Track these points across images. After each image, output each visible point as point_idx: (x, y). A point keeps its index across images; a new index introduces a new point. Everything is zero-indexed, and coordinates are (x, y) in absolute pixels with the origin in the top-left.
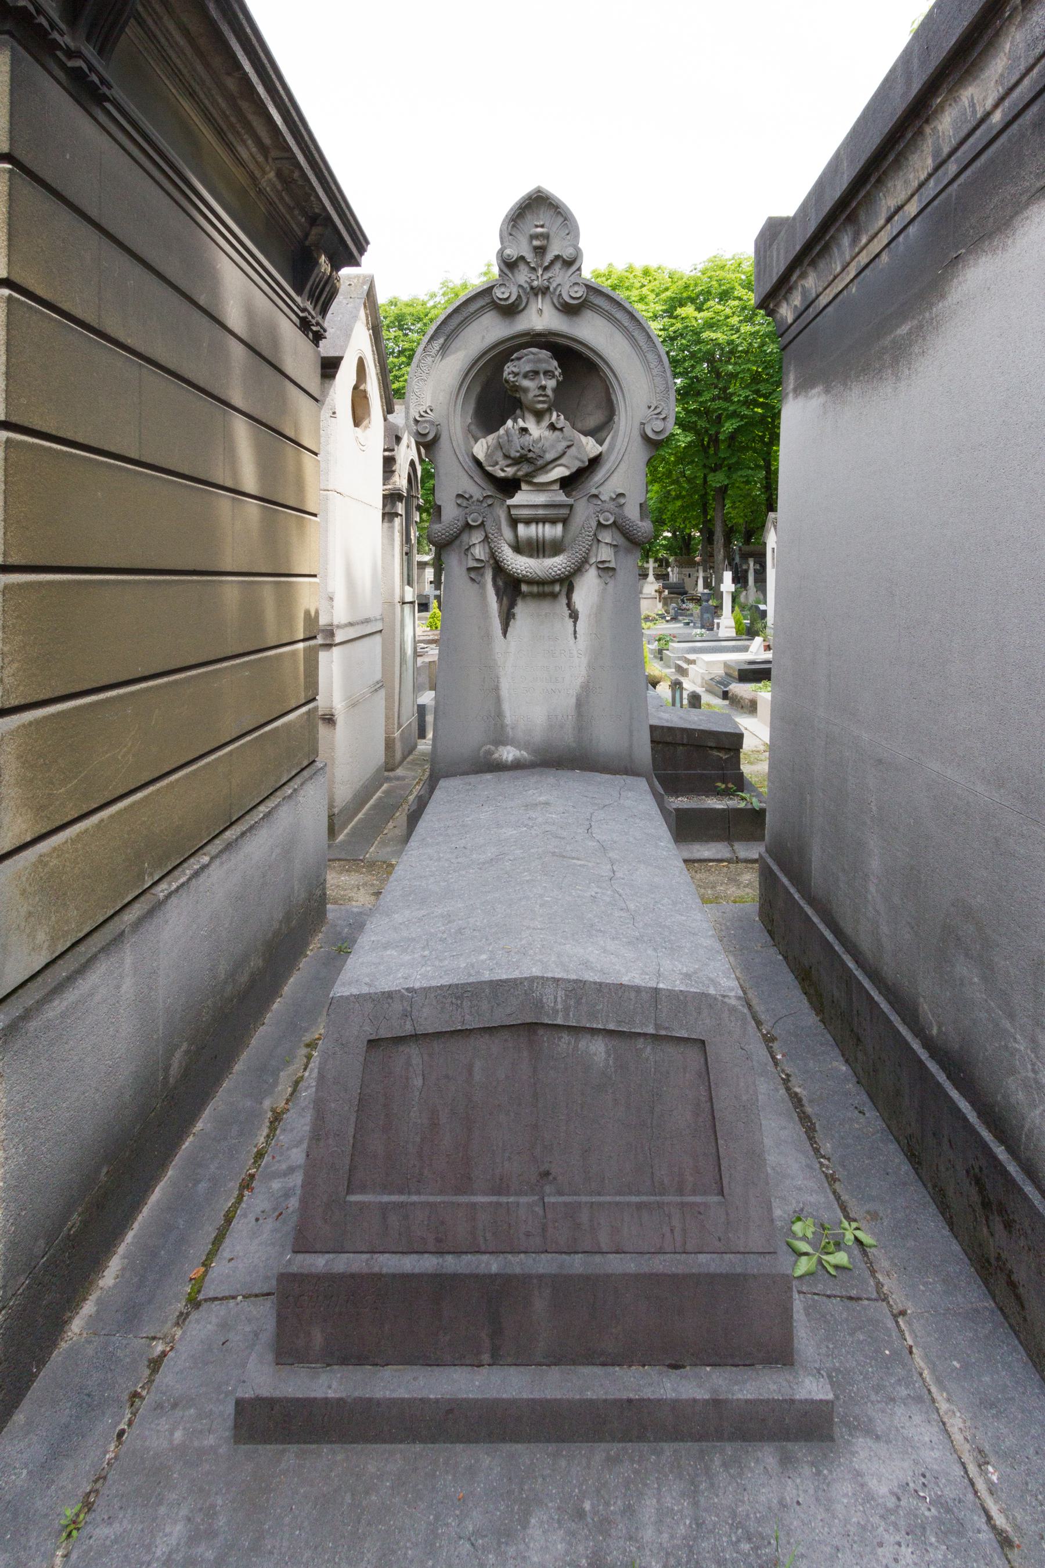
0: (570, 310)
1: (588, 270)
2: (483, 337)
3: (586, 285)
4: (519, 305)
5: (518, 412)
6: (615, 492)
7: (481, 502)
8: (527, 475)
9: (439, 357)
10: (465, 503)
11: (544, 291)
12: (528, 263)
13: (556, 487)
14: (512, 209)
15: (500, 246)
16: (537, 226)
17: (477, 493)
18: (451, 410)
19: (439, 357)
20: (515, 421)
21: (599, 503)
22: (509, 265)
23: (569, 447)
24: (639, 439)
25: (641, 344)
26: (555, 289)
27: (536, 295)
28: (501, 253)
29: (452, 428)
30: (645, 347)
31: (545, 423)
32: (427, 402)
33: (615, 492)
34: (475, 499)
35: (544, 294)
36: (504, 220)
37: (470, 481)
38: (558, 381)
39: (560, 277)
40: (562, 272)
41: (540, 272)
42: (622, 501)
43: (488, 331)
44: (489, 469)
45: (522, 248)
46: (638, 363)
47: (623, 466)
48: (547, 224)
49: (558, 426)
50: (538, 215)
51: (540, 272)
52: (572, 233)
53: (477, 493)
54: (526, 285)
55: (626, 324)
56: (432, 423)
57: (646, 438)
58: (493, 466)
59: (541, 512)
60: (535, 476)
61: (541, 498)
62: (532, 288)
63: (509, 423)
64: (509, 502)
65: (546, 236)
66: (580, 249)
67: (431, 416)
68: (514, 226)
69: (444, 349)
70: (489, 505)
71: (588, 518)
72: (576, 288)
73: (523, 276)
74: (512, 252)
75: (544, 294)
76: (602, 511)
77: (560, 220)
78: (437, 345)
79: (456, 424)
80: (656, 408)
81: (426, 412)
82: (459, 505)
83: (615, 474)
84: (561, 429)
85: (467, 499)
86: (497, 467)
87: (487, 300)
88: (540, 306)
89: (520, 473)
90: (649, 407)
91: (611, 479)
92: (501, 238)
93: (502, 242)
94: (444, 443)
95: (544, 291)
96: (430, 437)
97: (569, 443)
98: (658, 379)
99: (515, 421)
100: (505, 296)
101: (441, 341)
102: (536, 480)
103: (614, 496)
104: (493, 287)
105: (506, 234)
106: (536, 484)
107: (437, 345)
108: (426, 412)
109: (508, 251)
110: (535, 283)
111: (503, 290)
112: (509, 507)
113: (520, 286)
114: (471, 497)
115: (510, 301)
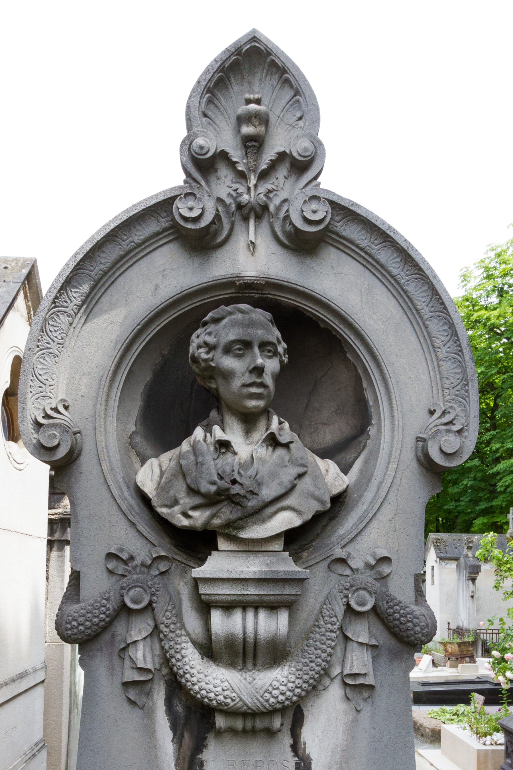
0: (303, 244)
1: (336, 179)
2: (157, 286)
3: (332, 203)
4: (216, 233)
5: (214, 414)
6: (374, 555)
7: (149, 567)
8: (229, 524)
9: (80, 317)
10: (121, 569)
11: (259, 212)
12: (233, 165)
13: (278, 546)
14: (207, 71)
15: (185, 133)
16: (248, 102)
17: (142, 552)
18: (101, 408)
19: (80, 317)
20: (208, 429)
21: (348, 572)
22: (202, 165)
23: (300, 476)
24: (414, 465)
25: (420, 305)
26: (278, 208)
27: (246, 219)
28: (187, 144)
29: (101, 438)
30: (426, 311)
31: (260, 434)
32: (60, 392)
33: (374, 555)
34: (138, 561)
35: (259, 218)
36: (194, 90)
37: (132, 532)
38: (281, 362)
39: (284, 189)
40: (289, 184)
41: (253, 180)
42: (386, 569)
43: (164, 276)
44: (163, 511)
45: (222, 138)
46: (413, 338)
47: (387, 512)
48: (265, 100)
49: (284, 439)
50: (250, 84)
51: (253, 180)
52: (307, 117)
53: (142, 552)
54: (228, 201)
55: (395, 272)
56: (65, 429)
57: (427, 464)
58: (170, 506)
59: (252, 590)
60: (242, 528)
61: (252, 567)
62: (240, 207)
63: (199, 433)
64: (198, 572)
65: (263, 119)
66: (320, 144)
67: (65, 417)
68: (210, 101)
69: (90, 304)
70: (162, 574)
71: (328, 600)
72: (314, 206)
73: (224, 185)
74: (208, 143)
75: (259, 218)
76: (354, 588)
77: (288, 94)
78: (77, 295)
79: (107, 432)
80: (444, 413)
81: (56, 410)
82: (111, 572)
83: (375, 524)
84: (287, 446)
85: (125, 562)
86: (177, 509)
87: (164, 223)
88: (252, 237)
89: (217, 522)
90: (432, 413)
91: (366, 532)
92: (189, 120)
93: (189, 128)
94: (87, 462)
95: (259, 212)
96: (61, 453)
97: (301, 470)
98: (447, 367)
99: (208, 429)
100: (195, 214)
101: (85, 288)
102: (244, 535)
103: (373, 562)
104: (173, 199)
105: (196, 114)
106: (243, 541)
107: (77, 295)
108: (56, 410)
109: (200, 141)
110: (245, 198)
111: (191, 203)
112: (196, 581)
113: (219, 200)
114: (132, 558)
115: (203, 223)
